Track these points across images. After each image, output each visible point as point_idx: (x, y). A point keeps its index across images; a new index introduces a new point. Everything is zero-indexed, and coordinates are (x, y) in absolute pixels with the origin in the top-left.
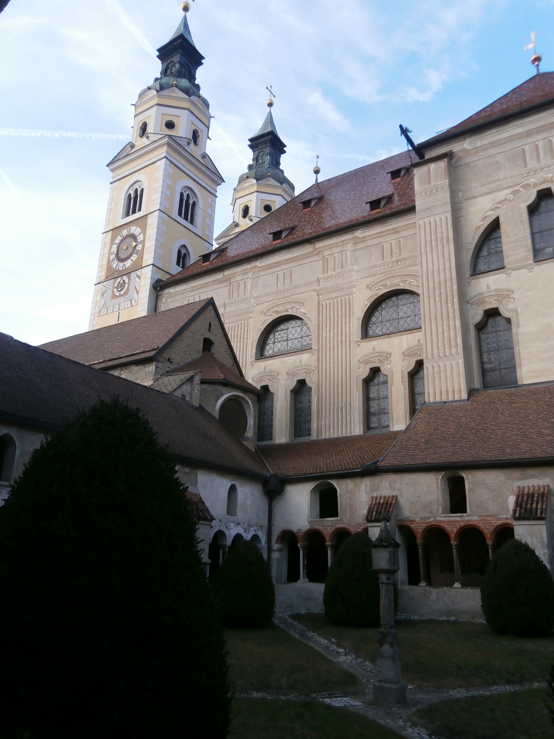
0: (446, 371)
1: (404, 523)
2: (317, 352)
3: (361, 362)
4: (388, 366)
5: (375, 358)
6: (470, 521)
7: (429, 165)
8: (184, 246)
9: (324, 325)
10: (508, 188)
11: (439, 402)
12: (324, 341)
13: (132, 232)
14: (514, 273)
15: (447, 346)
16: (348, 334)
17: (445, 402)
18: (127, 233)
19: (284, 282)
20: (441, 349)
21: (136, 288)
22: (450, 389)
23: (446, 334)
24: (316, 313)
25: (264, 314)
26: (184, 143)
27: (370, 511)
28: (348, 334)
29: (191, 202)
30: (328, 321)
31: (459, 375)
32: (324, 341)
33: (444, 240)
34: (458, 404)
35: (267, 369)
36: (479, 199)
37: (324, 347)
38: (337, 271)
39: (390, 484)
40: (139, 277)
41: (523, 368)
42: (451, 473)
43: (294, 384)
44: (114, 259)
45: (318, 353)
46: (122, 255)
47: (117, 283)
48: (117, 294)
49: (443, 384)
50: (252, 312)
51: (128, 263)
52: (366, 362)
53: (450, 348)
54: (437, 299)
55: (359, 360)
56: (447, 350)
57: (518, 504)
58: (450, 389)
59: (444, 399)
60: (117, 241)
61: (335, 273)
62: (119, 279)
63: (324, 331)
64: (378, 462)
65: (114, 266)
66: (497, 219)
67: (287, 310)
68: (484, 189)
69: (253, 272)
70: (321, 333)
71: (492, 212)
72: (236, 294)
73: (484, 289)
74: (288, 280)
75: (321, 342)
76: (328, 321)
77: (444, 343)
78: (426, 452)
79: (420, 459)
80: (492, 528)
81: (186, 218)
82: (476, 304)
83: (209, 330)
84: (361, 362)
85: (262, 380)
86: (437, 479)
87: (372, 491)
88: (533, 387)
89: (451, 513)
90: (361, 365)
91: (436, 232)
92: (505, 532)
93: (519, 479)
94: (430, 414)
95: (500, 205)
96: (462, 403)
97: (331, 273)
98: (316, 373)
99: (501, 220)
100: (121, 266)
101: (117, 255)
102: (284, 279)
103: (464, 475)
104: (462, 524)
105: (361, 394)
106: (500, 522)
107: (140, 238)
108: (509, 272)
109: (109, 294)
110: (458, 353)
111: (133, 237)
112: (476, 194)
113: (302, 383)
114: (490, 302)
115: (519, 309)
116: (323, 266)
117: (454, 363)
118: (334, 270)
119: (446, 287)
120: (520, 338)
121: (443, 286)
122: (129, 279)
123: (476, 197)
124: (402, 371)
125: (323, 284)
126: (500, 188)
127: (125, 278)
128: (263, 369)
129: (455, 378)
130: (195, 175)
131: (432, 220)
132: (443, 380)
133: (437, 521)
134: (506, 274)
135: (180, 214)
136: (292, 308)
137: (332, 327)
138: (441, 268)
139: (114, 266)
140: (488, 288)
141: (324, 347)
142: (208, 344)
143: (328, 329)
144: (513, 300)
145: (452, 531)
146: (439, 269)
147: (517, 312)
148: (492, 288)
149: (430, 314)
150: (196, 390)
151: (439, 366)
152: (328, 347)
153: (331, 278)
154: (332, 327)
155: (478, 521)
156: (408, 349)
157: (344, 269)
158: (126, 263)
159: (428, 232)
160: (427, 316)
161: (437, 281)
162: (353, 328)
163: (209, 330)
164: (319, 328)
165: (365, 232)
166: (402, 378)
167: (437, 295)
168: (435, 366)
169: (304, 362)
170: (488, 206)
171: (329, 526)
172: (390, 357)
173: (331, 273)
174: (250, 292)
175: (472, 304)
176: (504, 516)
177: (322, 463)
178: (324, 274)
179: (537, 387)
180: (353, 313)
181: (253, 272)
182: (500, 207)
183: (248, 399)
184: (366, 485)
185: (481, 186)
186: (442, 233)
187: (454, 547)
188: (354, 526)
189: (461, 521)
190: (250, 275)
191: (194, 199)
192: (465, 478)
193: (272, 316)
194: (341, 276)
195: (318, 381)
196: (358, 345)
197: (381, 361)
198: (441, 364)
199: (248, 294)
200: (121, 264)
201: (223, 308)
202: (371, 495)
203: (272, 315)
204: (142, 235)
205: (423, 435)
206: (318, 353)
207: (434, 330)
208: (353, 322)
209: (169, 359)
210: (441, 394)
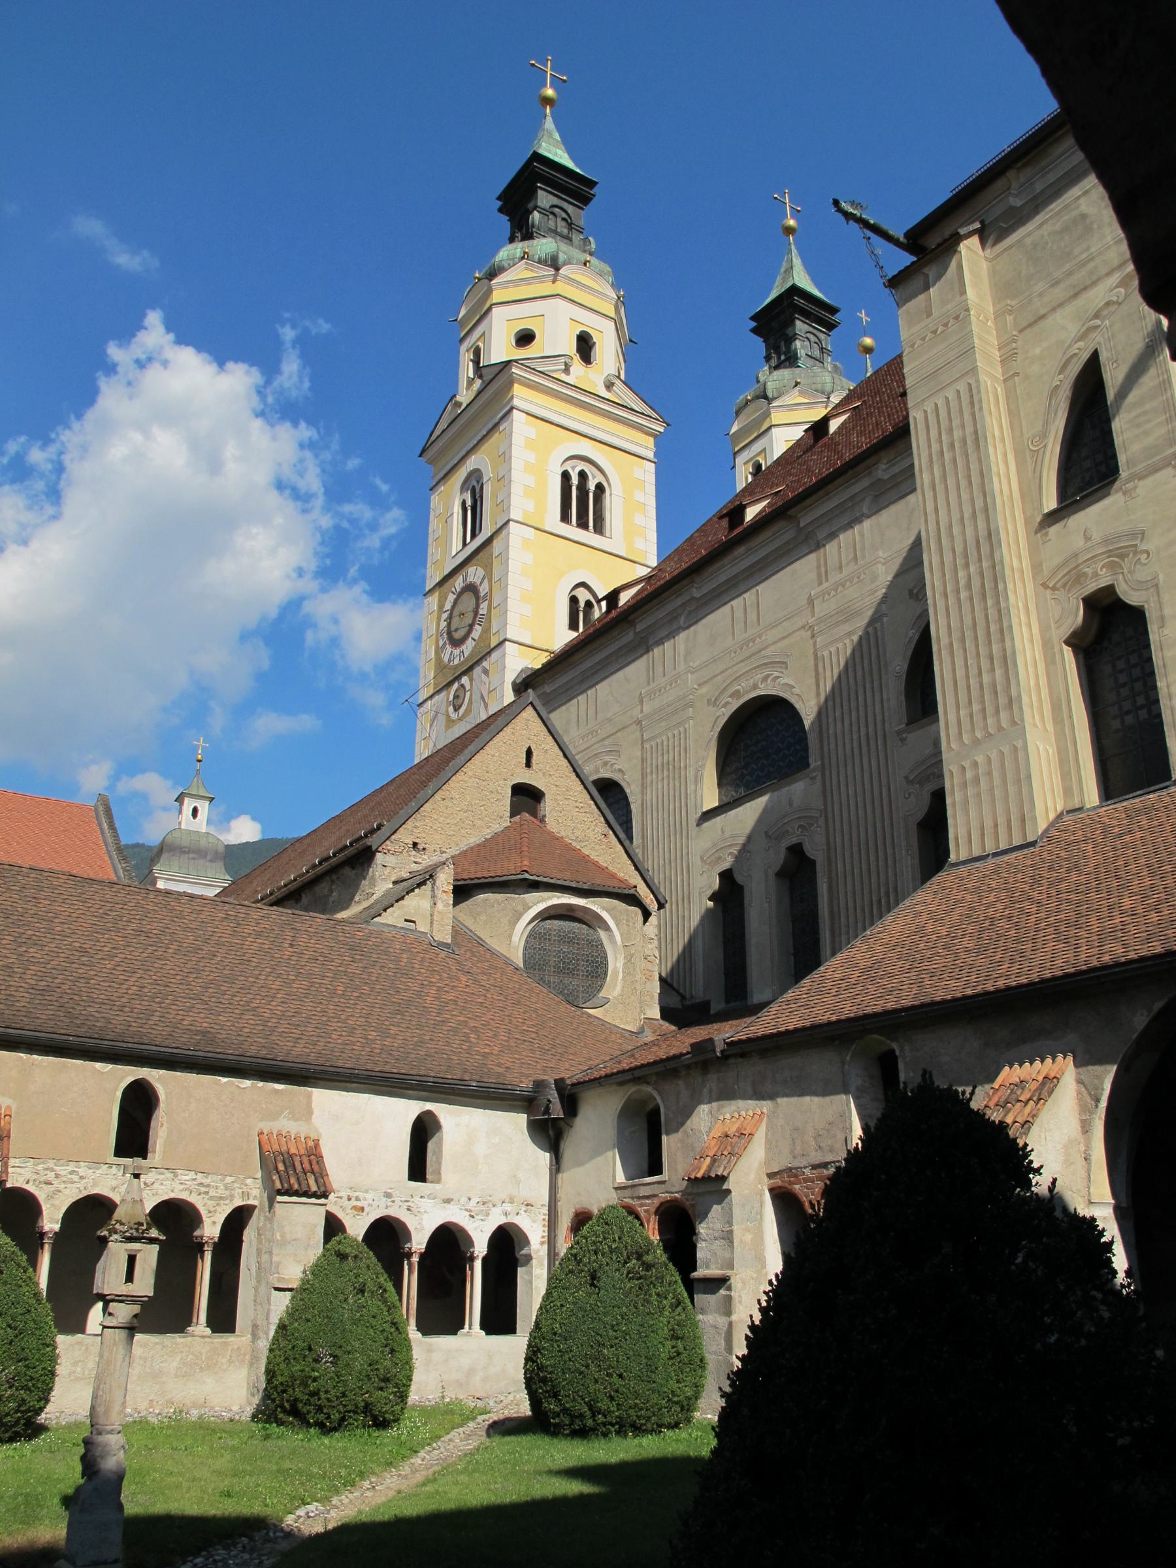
0: (989, 773)
7: (926, 270)
8: (583, 585)
10: (1109, 274)
12: (832, 746)
13: (470, 579)
14: (1142, 488)
16: (879, 718)
18: (462, 585)
19: (745, 622)
21: (482, 698)
23: (986, 678)
24: (814, 681)
25: (715, 704)
26: (555, 368)
28: (879, 718)
29: (592, 486)
32: (832, 746)
33: (969, 442)
35: (727, 834)
36: (1049, 321)
38: (845, 572)
40: (486, 672)
43: (782, 856)
44: (445, 643)
45: (823, 775)
46: (458, 635)
47: (452, 693)
48: (454, 716)
49: (986, 808)
50: (690, 705)
51: (468, 647)
53: (997, 712)
54: (964, 595)
55: (906, 778)
60: (448, 606)
61: (842, 576)
62: (456, 685)
63: (831, 720)
65: (446, 660)
66: (1095, 356)
67: (755, 687)
68: (1059, 293)
69: (686, 612)
70: (824, 727)
71: (1081, 344)
72: (659, 670)
73: (1079, 543)
74: (752, 616)
75: (826, 748)
81: (583, 525)
82: (1064, 586)
83: (528, 764)
84: (911, 782)
85: (720, 858)
86: (843, 1063)
91: (950, 430)
95: (1098, 322)
97: (834, 577)
99: (1103, 357)
100: (456, 657)
101: (449, 633)
102: (745, 613)
103: (895, 1046)
105: (917, 861)
107: (483, 589)
108: (1130, 485)
109: (441, 719)
111: (471, 588)
112: (1042, 312)
113: (796, 851)
114: (1096, 575)
116: (819, 567)
118: (841, 568)
119: (980, 560)
121: (973, 558)
122: (471, 680)
123: (1043, 317)
125: (821, 609)
126: (1094, 278)
127: (465, 680)
128: (720, 832)
130: (594, 427)
131: (941, 402)
134: (1124, 494)
135: (565, 517)
136: (765, 679)
138: (967, 515)
139: (446, 660)
140: (1088, 538)
142: (526, 797)
143: (838, 714)
144: (1145, 556)
146: (962, 519)
147: (1157, 586)
148: (1096, 536)
149: (950, 635)
150: (440, 906)
151: (975, 764)
152: (841, 758)
153: (836, 590)
157: (861, 562)
158: (464, 647)
159: (934, 433)
160: (944, 641)
161: (959, 549)
162: (888, 700)
163: (528, 764)
165: (894, 465)
167: (962, 583)
170: (1074, 329)
171: (647, 1197)
173: (834, 577)
174: (685, 660)
175: (1054, 589)
178: (820, 584)
181: (686, 612)
182: (1099, 326)
183: (599, 911)
185: (1053, 286)
186: (963, 426)
190: (682, 619)
191: (600, 478)
192: (897, 1053)
193: (729, 707)
194: (856, 580)
196: (902, 740)
198: (980, 759)
199: (681, 668)
200: (457, 652)
201: (639, 708)
203: (728, 703)
204: (486, 581)
206: (823, 775)
207: (960, 673)
209: (415, 845)
210: (983, 835)
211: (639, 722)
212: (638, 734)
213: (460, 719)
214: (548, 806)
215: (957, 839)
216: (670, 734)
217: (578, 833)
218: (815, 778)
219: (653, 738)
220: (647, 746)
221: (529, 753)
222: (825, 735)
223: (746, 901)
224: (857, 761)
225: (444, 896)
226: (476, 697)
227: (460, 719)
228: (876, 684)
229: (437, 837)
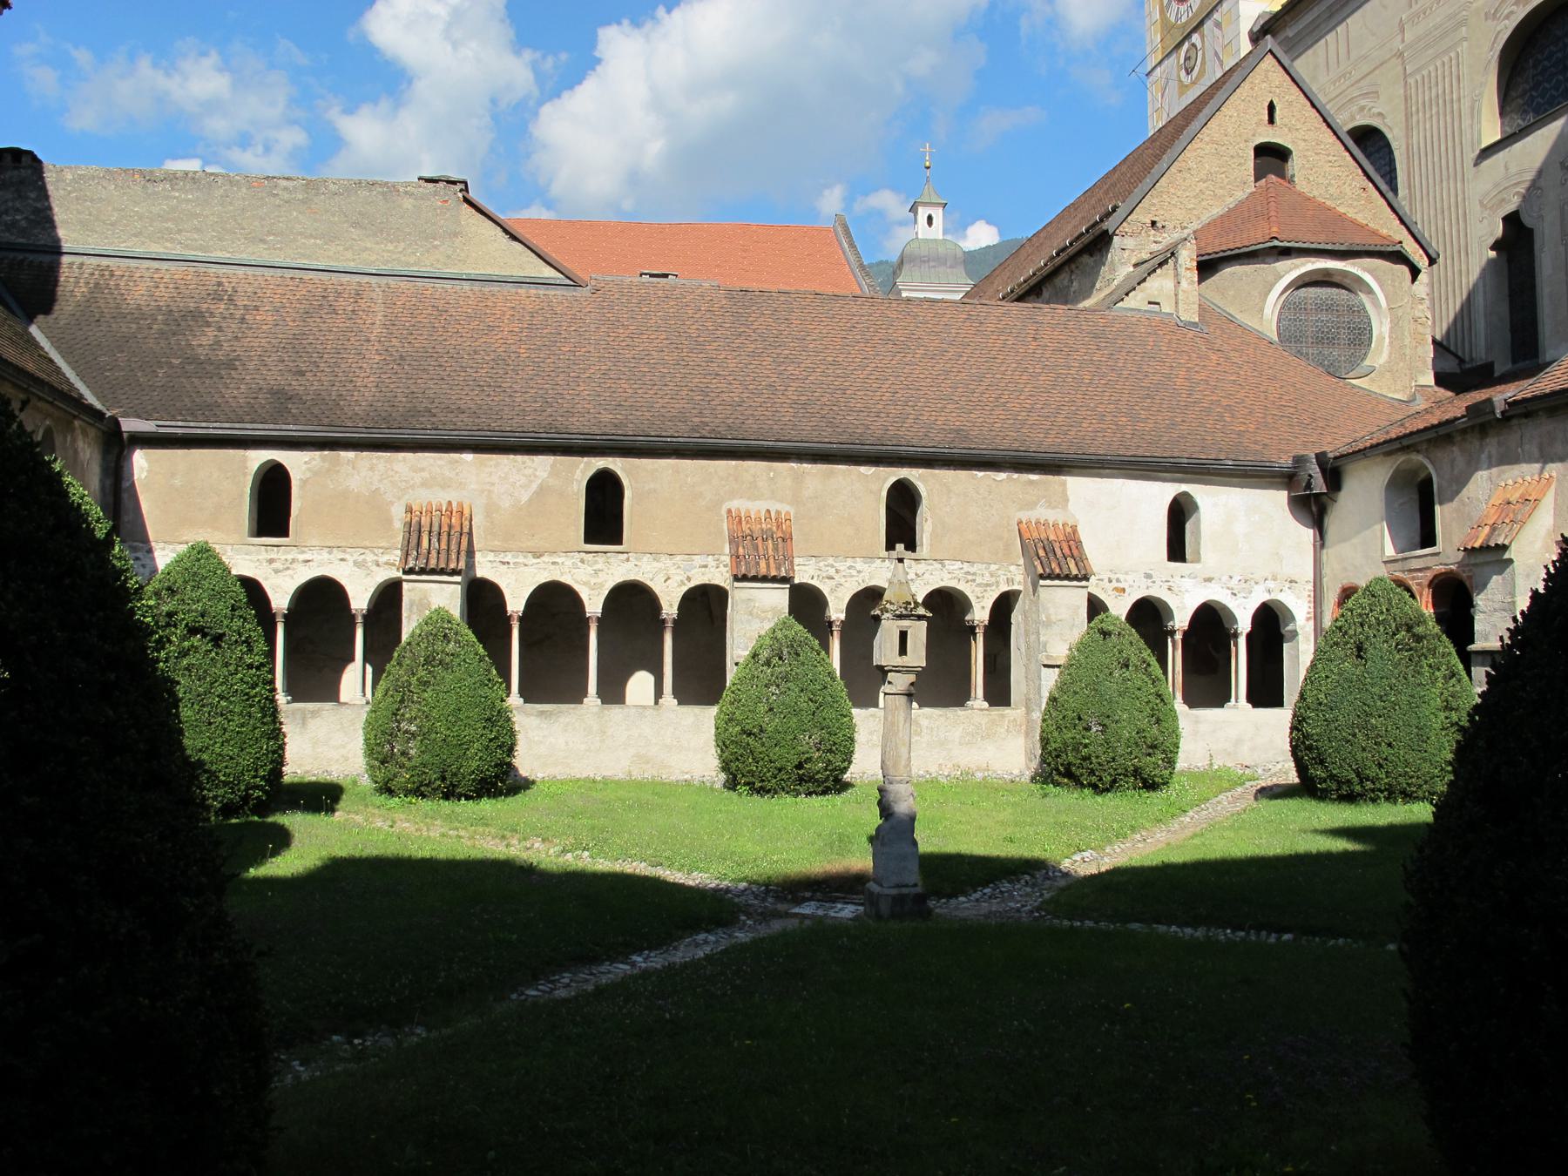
21: (1216, 54)
35: (1513, 170)
40: (1218, 25)
48: (1186, 80)
62: (1186, 45)
83: (1271, 120)
109: (1173, 85)
122: (1202, 37)
127: (1195, 38)
142: (1271, 157)
150: (1184, 284)
163: (1271, 120)
171: (1420, 570)
200: (1183, 8)
201: (1399, 38)
209: (1153, 223)
211: (1400, 55)
212: (1400, 68)
213: (1194, 83)
214: (1295, 165)
216: (1439, 63)
217: (1332, 190)
219: (1418, 70)
220: (1411, 81)
221: (1271, 108)
223: (1537, 246)
225: (1188, 274)
226: (1209, 55)
227: (1194, 83)
229: (1176, 211)
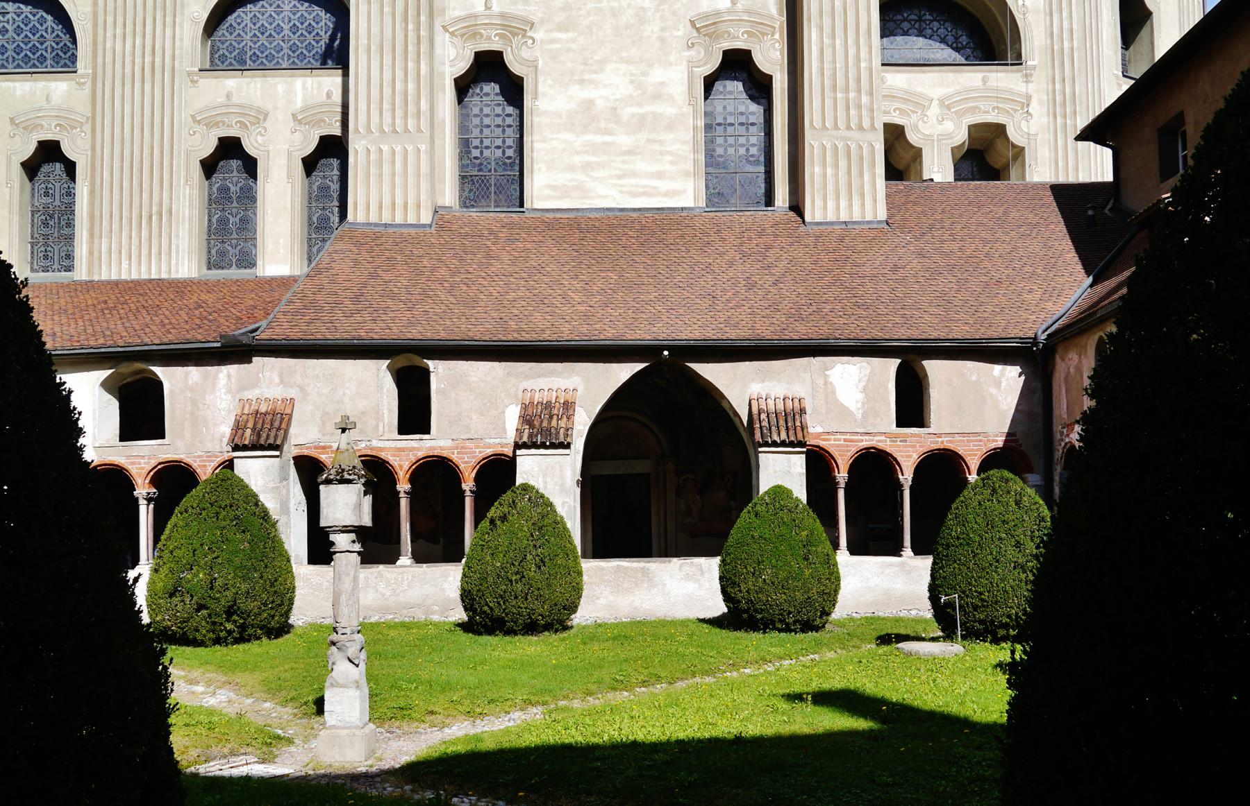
0: (393, 162)
1: (306, 452)
2: (89, 84)
3: (199, 122)
4: (259, 138)
5: (232, 116)
6: (434, 448)
9: (110, 19)
11: (376, 225)
12: (109, 60)
15: (399, 112)
16: (168, 53)
17: (386, 225)
20: (387, 115)
22: (399, 201)
23: (398, 86)
27: (238, 427)
28: (168, 53)
30: (120, 11)
31: (419, 175)
32: (109, 60)
34: (413, 231)
37: (109, 74)
39: (281, 376)
41: (535, 177)
42: (402, 361)
49: (386, 188)
52: (210, 124)
53: (406, 117)
56: (398, 121)
57: (526, 419)
58: (399, 201)
59: (386, 219)
63: (109, 34)
64: (256, 330)
70: (100, 38)
75: (100, 60)
76: (120, 11)
77: (393, 104)
78: (358, 317)
79: (344, 330)
80: (473, 462)
84: (199, 122)
87: (241, 389)
88: (551, 215)
89: (400, 433)
90: (197, 128)
92: (497, 473)
93: (527, 377)
94: (358, 244)
96: (418, 230)
98: (89, 131)
104: (421, 454)
106: (489, 451)
110: (419, 130)
115: (540, 62)
117: (410, 148)
120: (536, 120)
124: (290, 154)
129: (411, 180)
132: (386, 179)
133: (372, 449)
137: (129, 29)
141: (109, 74)
143: (119, 31)
145: (401, 466)
151: (381, 150)
154: (129, 29)
155: (450, 448)
156: (304, 110)
162: (181, 39)
164: (95, 25)
166: (289, 167)
168: (372, 149)
169: (55, 101)
171: (143, 457)
172: (265, 120)
176: (497, 441)
177: (120, 327)
179: (558, 215)
180: (182, 6)
184: (229, 376)
187: (402, 495)
188: (199, 456)
189: (418, 449)
195: (93, 149)
196: (192, 81)
197: (243, 126)
198: (385, 148)
202: (238, 398)
205: (348, 284)
208: (181, 27)
210: (381, 207)
215: (355, 204)
218: (84, 84)
222: (100, 47)
224: (138, 85)
228: (169, 20)
